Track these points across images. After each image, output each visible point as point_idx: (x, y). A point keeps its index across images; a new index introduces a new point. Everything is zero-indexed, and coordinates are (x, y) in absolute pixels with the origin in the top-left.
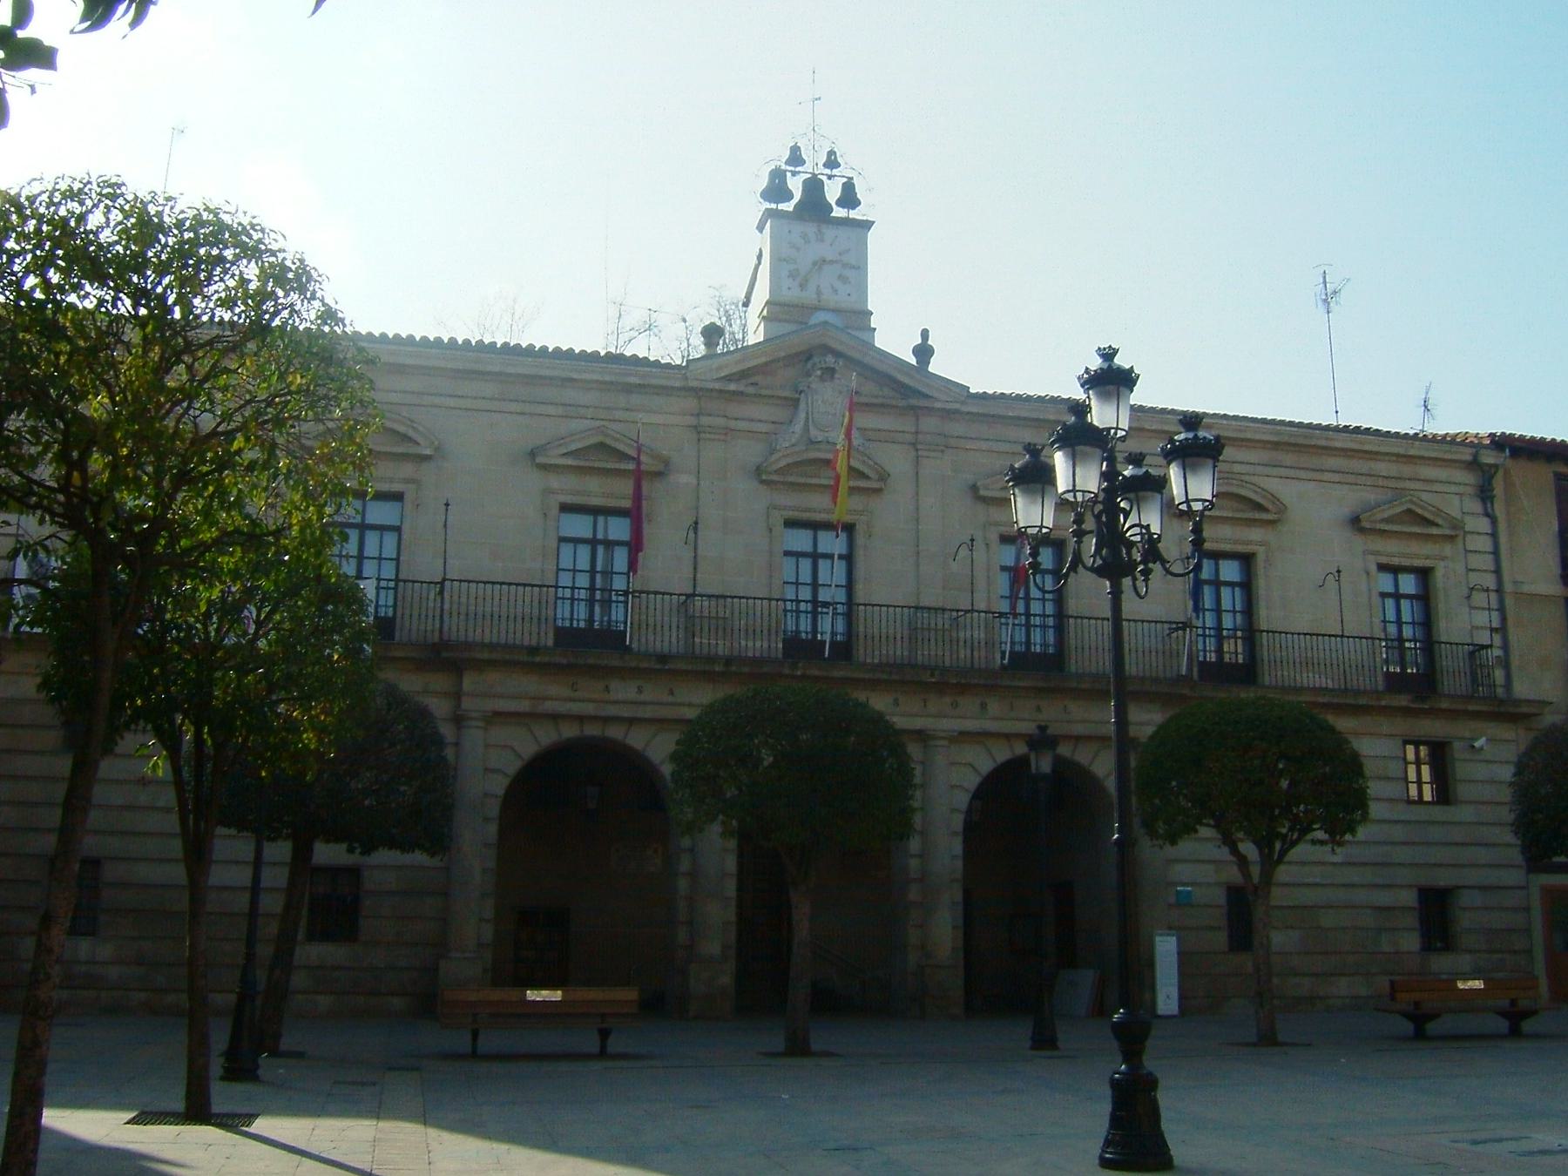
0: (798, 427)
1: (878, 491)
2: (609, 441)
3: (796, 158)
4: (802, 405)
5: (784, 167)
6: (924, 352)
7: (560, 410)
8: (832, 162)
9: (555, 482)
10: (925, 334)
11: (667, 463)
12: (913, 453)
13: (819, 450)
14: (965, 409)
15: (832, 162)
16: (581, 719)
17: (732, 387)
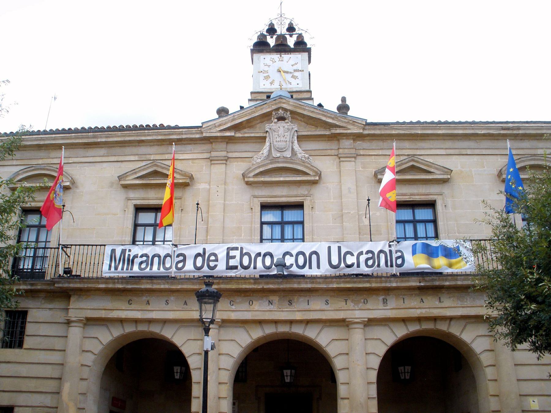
0: (265, 151)
1: (315, 183)
2: (159, 170)
3: (272, 30)
4: (267, 139)
5: (265, 33)
6: (343, 108)
7: (136, 158)
8: (291, 29)
9: (132, 194)
10: (344, 99)
11: (191, 178)
12: (338, 160)
13: (278, 162)
14: (366, 132)
15: (291, 29)
16: (136, 321)
17: (228, 134)
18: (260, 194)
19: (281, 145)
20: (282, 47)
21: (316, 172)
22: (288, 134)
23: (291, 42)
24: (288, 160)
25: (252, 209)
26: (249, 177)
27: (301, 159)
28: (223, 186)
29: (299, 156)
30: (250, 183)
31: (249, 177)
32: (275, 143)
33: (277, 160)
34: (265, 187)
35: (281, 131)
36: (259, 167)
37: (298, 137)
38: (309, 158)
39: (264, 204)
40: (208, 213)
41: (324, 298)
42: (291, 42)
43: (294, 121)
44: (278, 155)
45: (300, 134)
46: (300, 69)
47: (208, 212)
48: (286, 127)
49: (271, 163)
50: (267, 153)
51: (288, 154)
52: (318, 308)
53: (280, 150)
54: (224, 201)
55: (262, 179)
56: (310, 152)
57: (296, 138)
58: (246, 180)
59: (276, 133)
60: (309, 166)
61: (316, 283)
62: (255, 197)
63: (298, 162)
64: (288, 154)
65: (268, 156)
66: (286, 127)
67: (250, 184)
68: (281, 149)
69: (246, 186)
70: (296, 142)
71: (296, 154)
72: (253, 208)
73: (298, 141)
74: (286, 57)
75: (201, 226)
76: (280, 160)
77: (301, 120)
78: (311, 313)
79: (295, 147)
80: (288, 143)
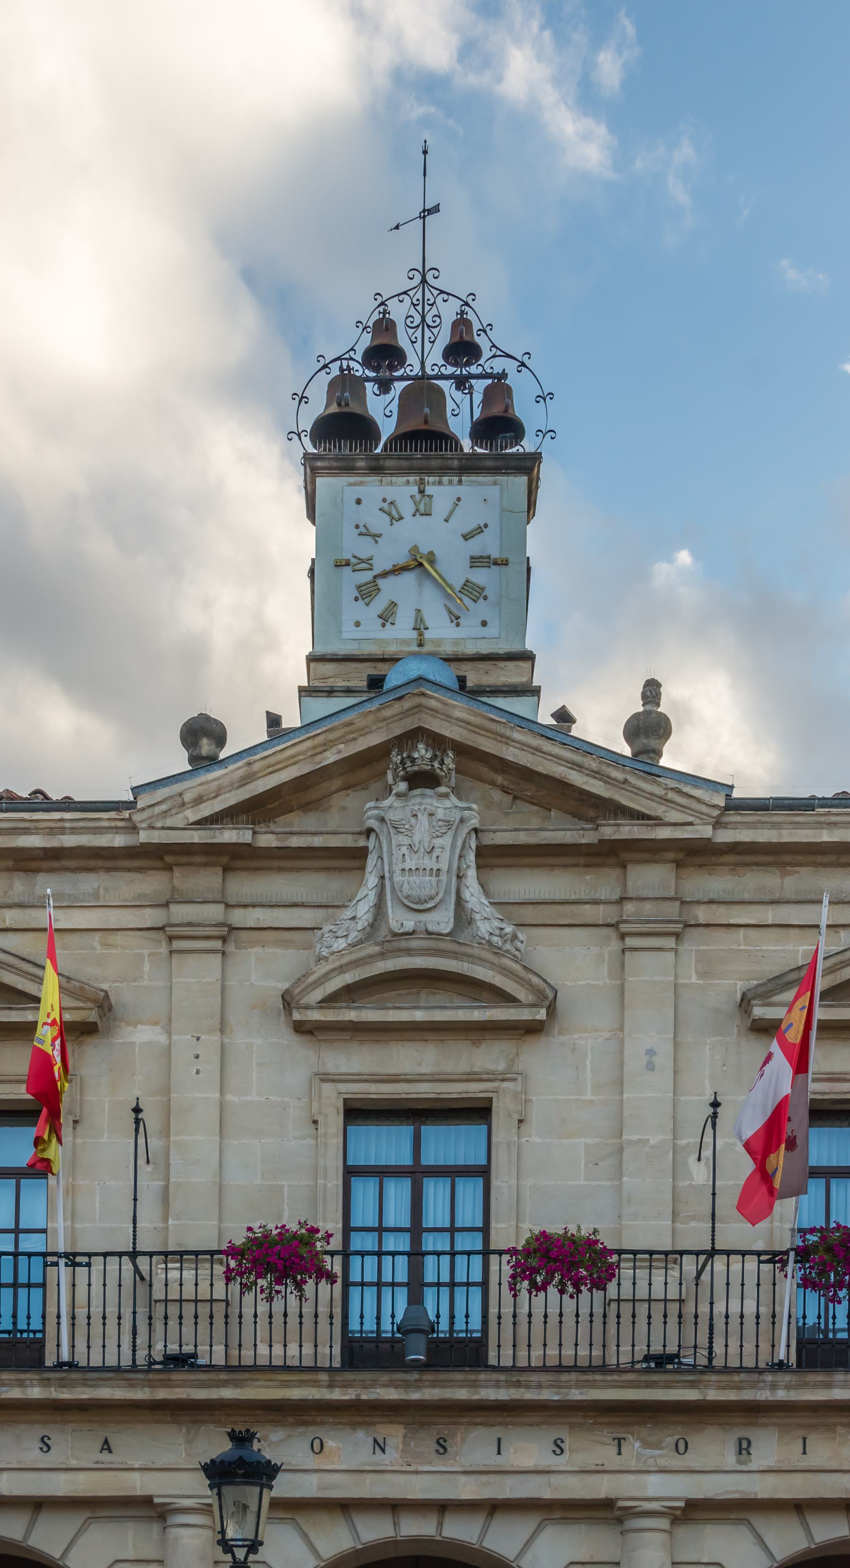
13: (409, 952)
18: (343, 1070)
19: (420, 885)
20: (423, 445)
21: (540, 995)
22: (447, 841)
23: (460, 414)
24: (442, 945)
25: (315, 1122)
26: (307, 1007)
27: (489, 942)
28: (216, 1037)
29: (483, 928)
30: (308, 1027)
31: (307, 1007)
32: (398, 878)
33: (403, 944)
34: (362, 1042)
35: (422, 830)
36: (342, 969)
37: (481, 852)
38: (515, 937)
39: (357, 1105)
40: (168, 1136)
41: (549, 1434)
42: (460, 414)
43: (468, 783)
44: (409, 926)
45: (489, 839)
46: (495, 554)
47: (166, 1132)
48: (440, 814)
49: (383, 955)
50: (369, 917)
51: (442, 920)
52: (528, 1463)
53: (418, 906)
54: (222, 1092)
55: (351, 1015)
56: (523, 910)
57: (471, 857)
58: (297, 1016)
59: (397, 839)
60: (516, 967)
61: (528, 1387)
62: (326, 1078)
63: (477, 952)
64: (442, 920)
65: (372, 926)
66: (440, 814)
67: (311, 1032)
68: (420, 902)
69: (295, 1038)
70: (472, 873)
71: (470, 922)
72: (321, 1120)
73: (479, 867)
74: (442, 492)
75: (149, 1184)
76: (414, 944)
77: (493, 783)
78: (509, 1480)
79: (466, 894)
80: (444, 877)
